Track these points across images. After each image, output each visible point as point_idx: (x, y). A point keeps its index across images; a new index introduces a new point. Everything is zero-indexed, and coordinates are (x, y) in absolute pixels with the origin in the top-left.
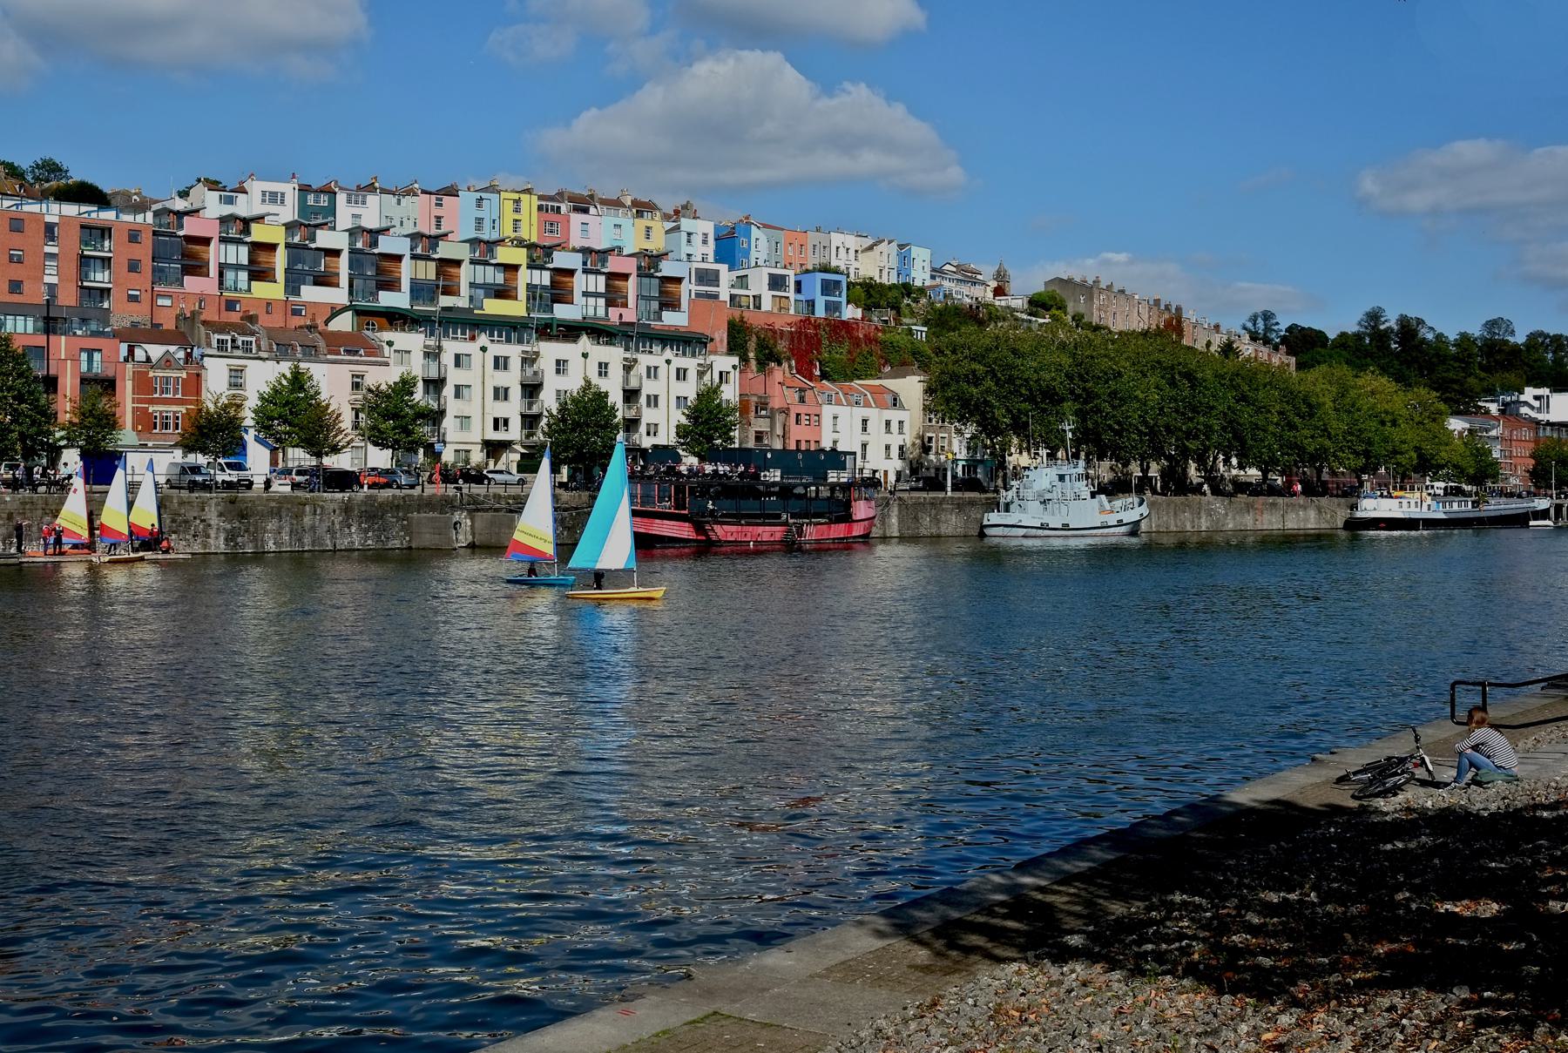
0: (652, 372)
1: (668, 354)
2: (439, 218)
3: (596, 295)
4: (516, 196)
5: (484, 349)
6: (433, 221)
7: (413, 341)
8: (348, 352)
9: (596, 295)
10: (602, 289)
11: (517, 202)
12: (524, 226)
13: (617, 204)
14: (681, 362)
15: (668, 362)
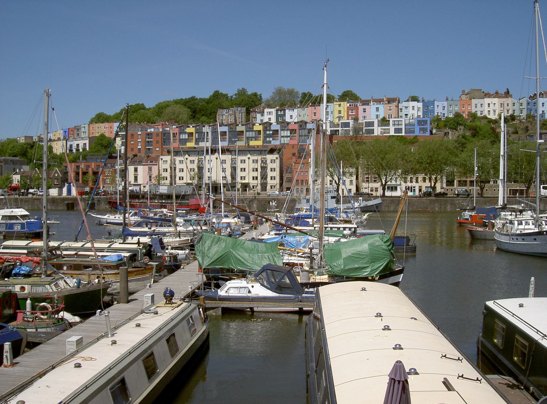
0: (243, 161)
1: (249, 156)
2: (315, 113)
3: (287, 137)
4: (339, 103)
5: (187, 159)
6: (313, 114)
7: (168, 158)
8: (151, 162)
9: (287, 137)
10: (289, 134)
11: (340, 105)
12: (342, 112)
13: (379, 101)
14: (255, 158)
15: (249, 158)
